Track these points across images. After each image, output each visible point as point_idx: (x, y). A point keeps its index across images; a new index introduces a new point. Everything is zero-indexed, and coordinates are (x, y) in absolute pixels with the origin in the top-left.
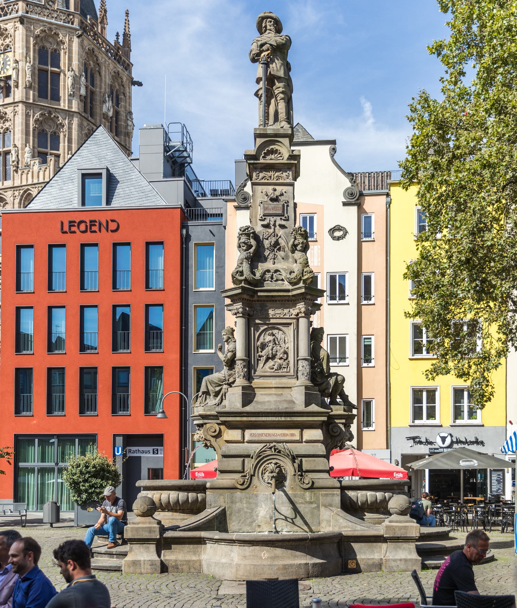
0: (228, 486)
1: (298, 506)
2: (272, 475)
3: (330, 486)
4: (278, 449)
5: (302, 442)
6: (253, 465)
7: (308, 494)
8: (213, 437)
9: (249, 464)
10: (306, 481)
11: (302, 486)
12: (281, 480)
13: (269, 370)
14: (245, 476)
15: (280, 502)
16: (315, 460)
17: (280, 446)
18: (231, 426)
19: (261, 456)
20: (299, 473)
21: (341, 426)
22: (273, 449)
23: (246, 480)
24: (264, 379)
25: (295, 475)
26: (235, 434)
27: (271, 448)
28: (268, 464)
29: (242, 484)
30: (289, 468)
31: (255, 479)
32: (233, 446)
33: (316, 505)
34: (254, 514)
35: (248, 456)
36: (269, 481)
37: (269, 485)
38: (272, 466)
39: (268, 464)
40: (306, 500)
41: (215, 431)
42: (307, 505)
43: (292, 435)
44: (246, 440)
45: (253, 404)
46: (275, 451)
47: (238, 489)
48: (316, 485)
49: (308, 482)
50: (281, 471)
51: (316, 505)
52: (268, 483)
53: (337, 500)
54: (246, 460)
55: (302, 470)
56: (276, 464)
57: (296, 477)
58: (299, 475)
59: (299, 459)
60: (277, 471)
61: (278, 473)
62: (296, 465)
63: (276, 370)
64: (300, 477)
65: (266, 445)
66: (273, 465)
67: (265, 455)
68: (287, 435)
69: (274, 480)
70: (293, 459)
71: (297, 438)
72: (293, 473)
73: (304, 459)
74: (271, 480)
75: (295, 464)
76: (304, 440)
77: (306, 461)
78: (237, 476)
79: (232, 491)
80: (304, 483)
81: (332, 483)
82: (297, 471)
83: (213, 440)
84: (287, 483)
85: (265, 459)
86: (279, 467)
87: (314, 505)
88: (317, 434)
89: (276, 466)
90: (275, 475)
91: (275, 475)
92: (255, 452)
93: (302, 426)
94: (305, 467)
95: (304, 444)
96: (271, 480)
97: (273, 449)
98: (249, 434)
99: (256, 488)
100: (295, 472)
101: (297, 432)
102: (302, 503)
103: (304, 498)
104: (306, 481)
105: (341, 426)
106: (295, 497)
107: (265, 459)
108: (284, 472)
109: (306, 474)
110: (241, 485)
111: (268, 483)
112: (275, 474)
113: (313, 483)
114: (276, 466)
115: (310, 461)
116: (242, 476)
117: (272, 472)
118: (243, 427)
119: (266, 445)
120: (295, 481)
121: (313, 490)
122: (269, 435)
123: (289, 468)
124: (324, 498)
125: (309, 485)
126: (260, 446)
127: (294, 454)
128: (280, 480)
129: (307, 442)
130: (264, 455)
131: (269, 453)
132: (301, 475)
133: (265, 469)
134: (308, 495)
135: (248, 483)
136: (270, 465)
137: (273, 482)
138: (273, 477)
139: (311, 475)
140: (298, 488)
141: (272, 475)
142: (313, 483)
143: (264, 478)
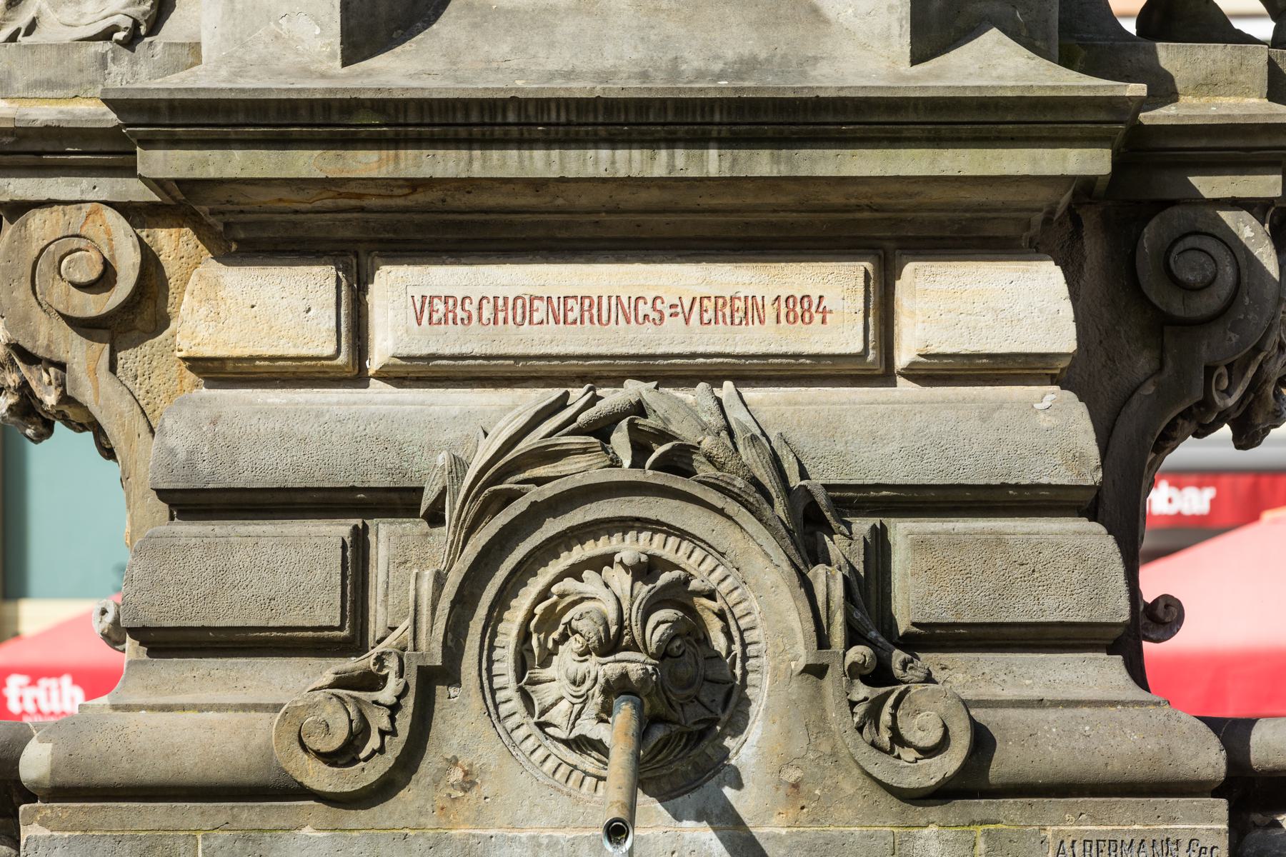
0: (218, 773)
2: (609, 668)
3: (1140, 771)
4: (663, 436)
5: (886, 376)
6: (440, 580)
8: (86, 327)
9: (411, 571)
10: (921, 729)
11: (881, 767)
12: (692, 715)
14: (372, 681)
16: (999, 539)
17: (685, 411)
18: (251, 232)
19: (510, 497)
20: (858, 653)
21: (1248, 230)
22: (620, 440)
23: (380, 720)
25: (816, 671)
26: (283, 306)
27: (602, 430)
28: (575, 572)
29: (344, 756)
30: (765, 607)
31: (459, 712)
32: (267, 412)
35: (399, 501)
36: (589, 727)
37: (588, 763)
38: (606, 595)
39: (575, 572)
41: (106, 279)
43: (800, 309)
44: (381, 352)
45: (447, 28)
46: (640, 451)
47: (301, 792)
48: (1003, 765)
49: (932, 737)
50: (690, 632)
52: (581, 744)
54: (385, 536)
55: (886, 621)
56: (646, 569)
57: (832, 684)
58: (855, 672)
59: (862, 526)
60: (655, 636)
61: (664, 654)
62: (829, 582)
64: (862, 691)
65: (561, 404)
66: (620, 580)
67: (549, 490)
68: (752, 310)
69: (624, 713)
70: (808, 519)
71: (844, 335)
72: (802, 652)
73: (901, 530)
74: (605, 714)
75: (818, 574)
76: (903, 357)
77: (920, 544)
78: (299, 681)
79: (249, 813)
80: (898, 739)
82: (838, 635)
83: (83, 356)
84: (749, 749)
85: (552, 527)
86: (679, 595)
88: (1027, 304)
89: (643, 590)
90: (635, 671)
91: (635, 671)
92: (459, 465)
93: (890, 235)
94: (909, 604)
95: (905, 387)
96: (605, 714)
97: (620, 440)
98: (404, 302)
99: (468, 783)
100: (823, 641)
101: (838, 285)
104: (921, 729)
105: (1248, 230)
107: (552, 527)
108: (719, 642)
109: (928, 660)
110: (331, 758)
111: (581, 744)
112: (635, 665)
113: (982, 741)
114: (643, 590)
115: (955, 542)
116: (342, 682)
117: (609, 645)
118: (355, 238)
119: (561, 404)
120: (819, 726)
121: (980, 807)
122: (591, 309)
123: (765, 607)
125: (949, 763)
126: (510, 408)
127: (817, 480)
128: (681, 717)
129: (939, 371)
130: (536, 494)
131: (581, 469)
132: (879, 675)
133: (550, 619)
136: (591, 583)
137: (618, 732)
138: (617, 688)
139: (964, 674)
140: (850, 784)
141: (609, 668)
142: (982, 741)
143: (543, 695)
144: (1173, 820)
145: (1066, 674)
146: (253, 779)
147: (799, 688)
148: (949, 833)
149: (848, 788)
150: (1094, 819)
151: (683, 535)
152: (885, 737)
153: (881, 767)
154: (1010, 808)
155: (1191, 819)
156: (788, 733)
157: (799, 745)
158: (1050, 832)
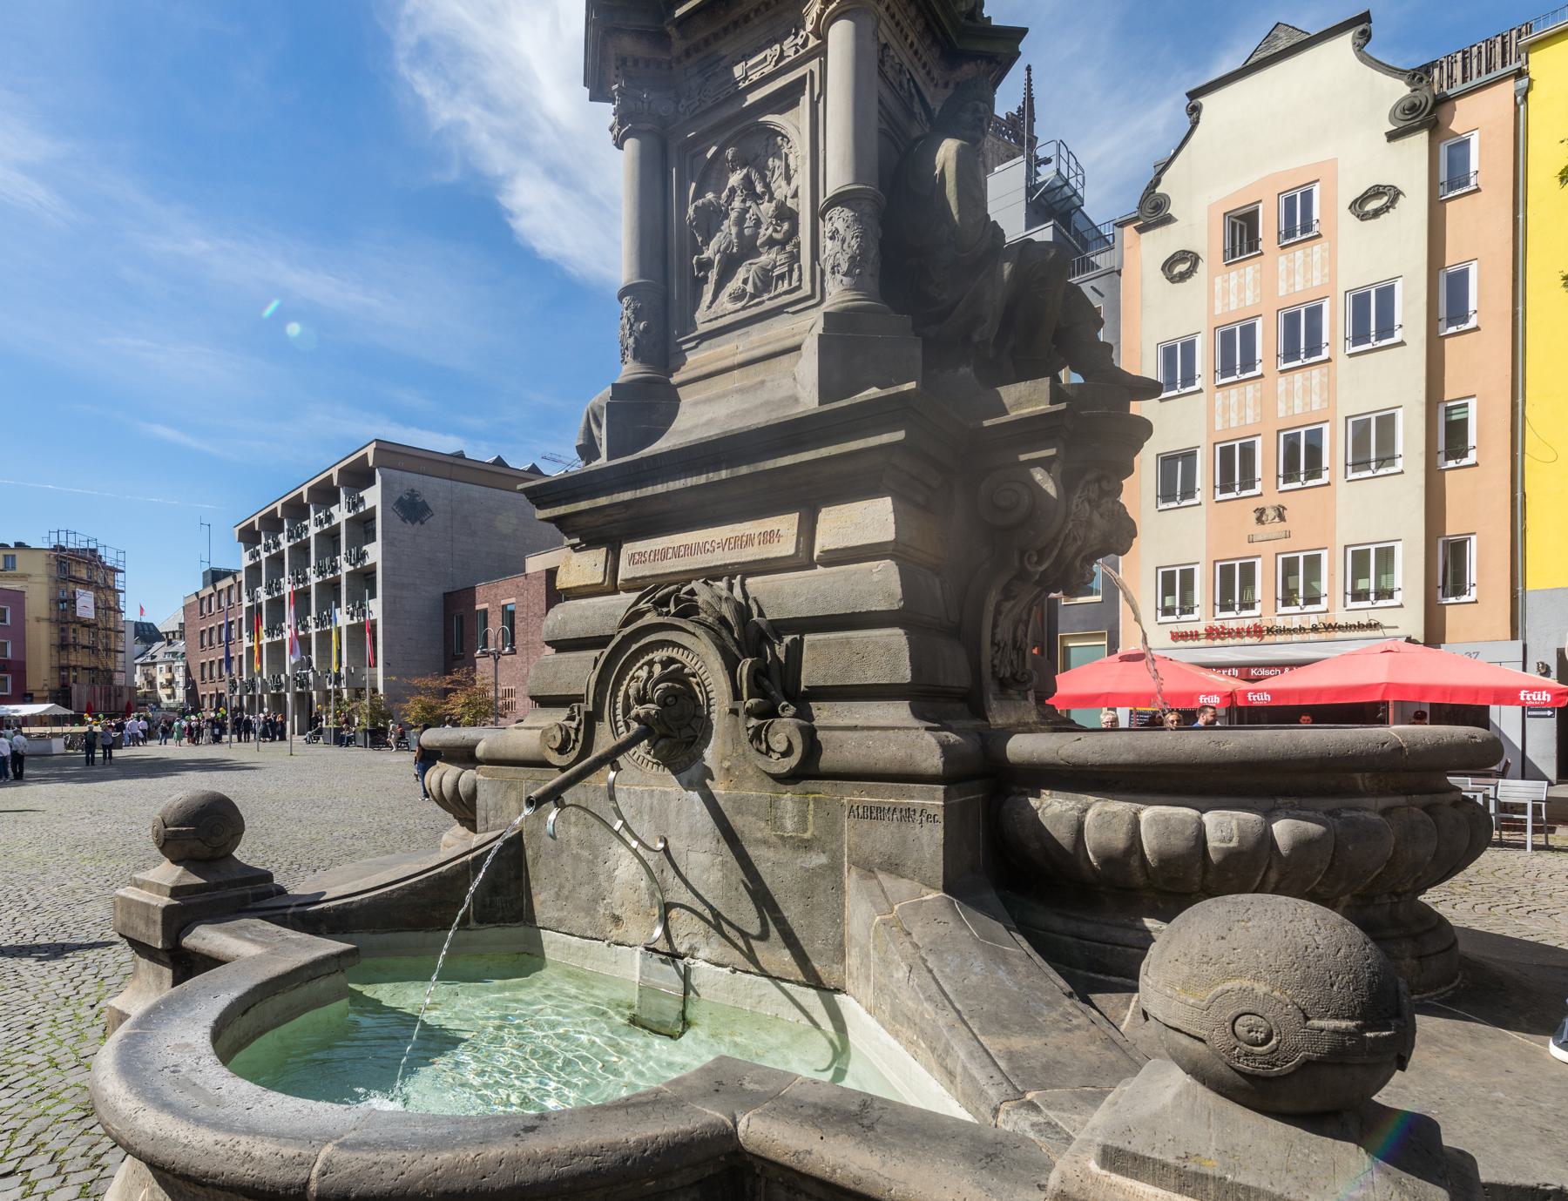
1: (752, 851)
7: (789, 799)
10: (779, 743)
13: (731, 307)
15: (685, 828)
24: (710, 348)
33: (823, 859)
34: (600, 869)
40: (782, 827)
42: (785, 854)
48: (827, 760)
49: (783, 747)
51: (823, 859)
53: (929, 840)
63: (753, 297)
68: (749, 540)
80: (769, 748)
81: (902, 753)
87: (818, 859)
102: (765, 842)
103: (776, 823)
106: (739, 812)
122: (689, 550)
124: (865, 823)
125: (793, 761)
134: (790, 805)
135: (578, 746)
144: (912, 797)
145: (878, 712)
146: (530, 757)
147: (728, 720)
148: (797, 798)
149: (750, 772)
150: (869, 795)
151: (680, 646)
152: (764, 747)
153: (761, 762)
154: (825, 786)
155: (922, 798)
156: (724, 743)
157: (730, 747)
158: (846, 799)
